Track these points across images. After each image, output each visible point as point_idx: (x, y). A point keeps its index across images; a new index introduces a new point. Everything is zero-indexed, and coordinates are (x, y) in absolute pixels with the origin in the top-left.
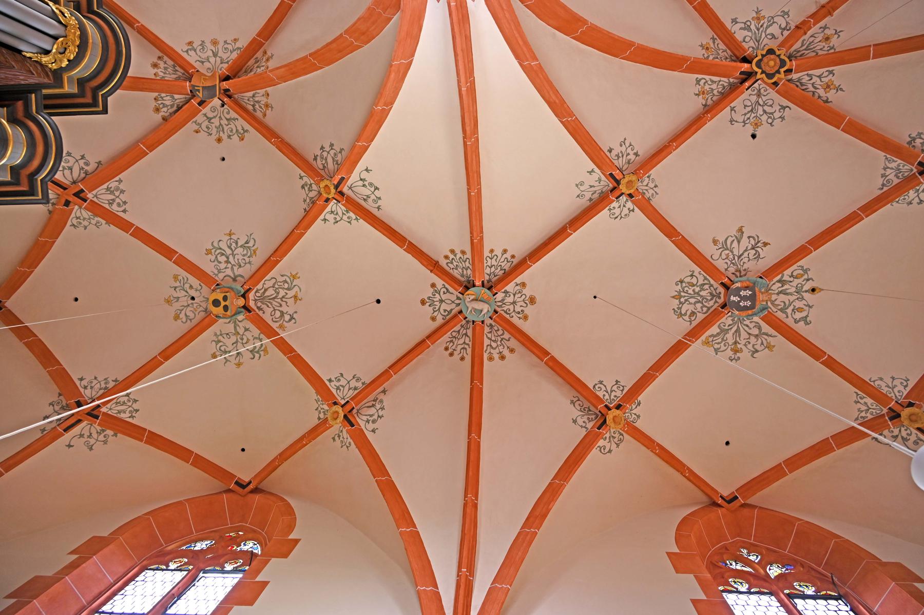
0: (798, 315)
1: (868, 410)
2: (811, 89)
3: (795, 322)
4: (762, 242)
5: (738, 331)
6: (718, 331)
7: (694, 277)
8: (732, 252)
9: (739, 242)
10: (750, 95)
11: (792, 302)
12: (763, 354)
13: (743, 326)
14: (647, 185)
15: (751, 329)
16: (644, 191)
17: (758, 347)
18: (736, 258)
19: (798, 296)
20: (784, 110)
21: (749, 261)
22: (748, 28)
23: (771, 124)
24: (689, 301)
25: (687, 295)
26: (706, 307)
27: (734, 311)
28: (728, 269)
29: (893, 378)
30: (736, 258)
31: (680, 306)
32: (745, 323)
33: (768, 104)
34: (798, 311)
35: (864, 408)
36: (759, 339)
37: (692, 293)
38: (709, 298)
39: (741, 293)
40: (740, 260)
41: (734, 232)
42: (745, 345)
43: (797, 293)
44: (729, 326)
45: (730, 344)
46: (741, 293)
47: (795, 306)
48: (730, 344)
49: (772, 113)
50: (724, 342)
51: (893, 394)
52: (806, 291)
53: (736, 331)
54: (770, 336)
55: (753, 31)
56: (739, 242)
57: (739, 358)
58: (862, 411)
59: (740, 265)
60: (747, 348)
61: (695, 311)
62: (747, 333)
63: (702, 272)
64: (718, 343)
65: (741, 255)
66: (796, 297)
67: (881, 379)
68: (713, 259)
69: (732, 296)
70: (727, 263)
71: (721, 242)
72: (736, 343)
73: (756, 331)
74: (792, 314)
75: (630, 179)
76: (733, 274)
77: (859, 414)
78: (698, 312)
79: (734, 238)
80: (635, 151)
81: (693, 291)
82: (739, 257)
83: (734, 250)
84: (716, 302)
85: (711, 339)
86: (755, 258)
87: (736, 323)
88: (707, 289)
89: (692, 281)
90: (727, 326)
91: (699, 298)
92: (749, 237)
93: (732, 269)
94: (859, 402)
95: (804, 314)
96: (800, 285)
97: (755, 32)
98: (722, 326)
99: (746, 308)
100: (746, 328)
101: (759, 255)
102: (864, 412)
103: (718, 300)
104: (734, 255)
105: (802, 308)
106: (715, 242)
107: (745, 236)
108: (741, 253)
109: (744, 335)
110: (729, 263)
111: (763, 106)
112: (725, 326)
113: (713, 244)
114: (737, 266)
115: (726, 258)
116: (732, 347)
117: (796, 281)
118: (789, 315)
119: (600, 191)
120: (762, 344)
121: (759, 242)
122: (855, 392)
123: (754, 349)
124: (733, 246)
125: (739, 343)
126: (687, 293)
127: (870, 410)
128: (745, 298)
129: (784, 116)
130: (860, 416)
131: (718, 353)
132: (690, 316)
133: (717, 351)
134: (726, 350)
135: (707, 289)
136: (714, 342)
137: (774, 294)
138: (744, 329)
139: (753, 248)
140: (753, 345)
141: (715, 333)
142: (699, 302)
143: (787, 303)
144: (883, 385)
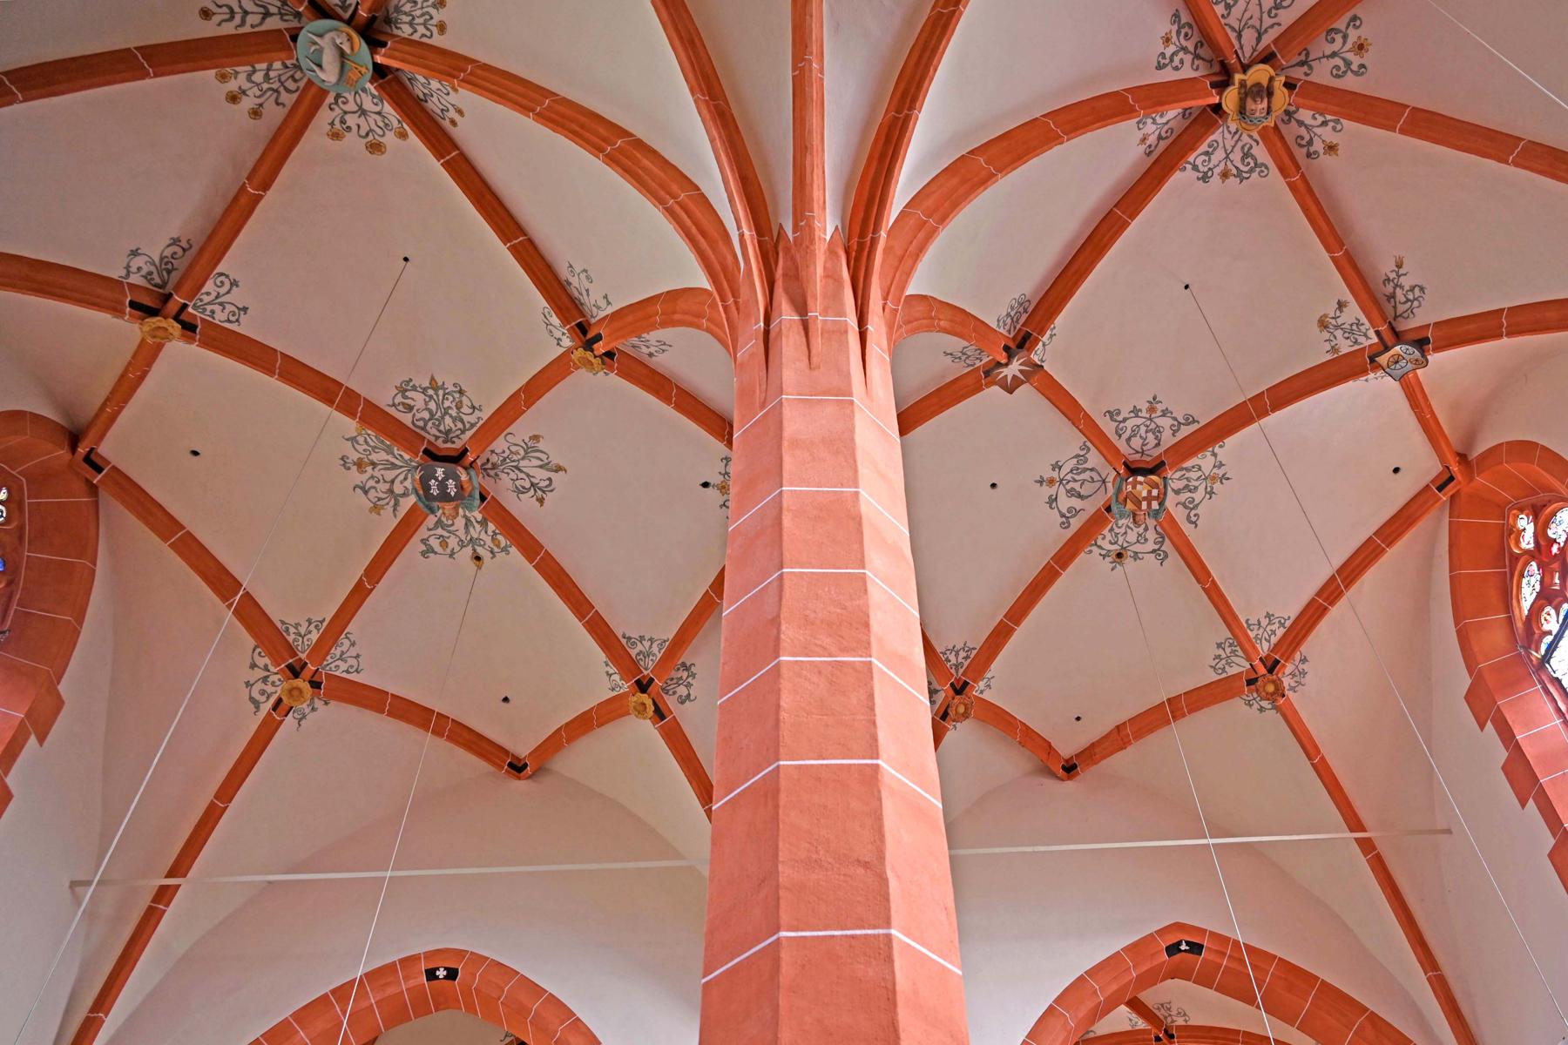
0: (435, 543)
1: (300, 636)
5: (394, 466)
12: (364, 502)
15: (401, 483)
17: (372, 494)
24: (430, 401)
25: (441, 398)
26: (425, 425)
27: (420, 472)
29: (358, 656)
31: (418, 389)
35: (302, 630)
36: (386, 496)
37: (445, 406)
38: (442, 428)
39: (451, 481)
42: (372, 477)
46: (451, 481)
51: (330, 661)
53: (392, 464)
54: (395, 510)
57: (349, 469)
58: (296, 628)
61: (415, 410)
63: (481, 422)
67: (353, 644)
72: (374, 465)
73: (398, 489)
77: (292, 625)
78: (414, 415)
81: (449, 408)
84: (437, 438)
88: (456, 426)
89: (465, 407)
91: (439, 414)
94: (310, 624)
99: (427, 488)
100: (402, 477)
102: (295, 631)
103: (441, 440)
109: (390, 475)
118: (432, 532)
119: (582, 301)
120: (380, 499)
122: (324, 619)
123: (369, 489)
126: (443, 399)
127: (300, 639)
128: (442, 485)
130: (290, 627)
132: (403, 404)
135: (456, 426)
138: (399, 474)
140: (374, 488)
142: (432, 415)
143: (451, 529)
144: (344, 648)
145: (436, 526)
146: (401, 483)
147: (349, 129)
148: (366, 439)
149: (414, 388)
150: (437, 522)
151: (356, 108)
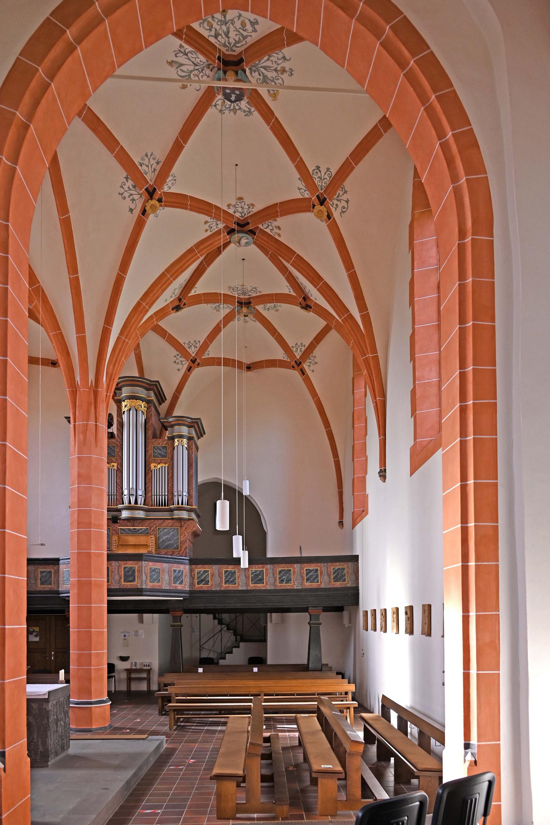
0: (249, 27)
3: (255, 32)
7: (217, 103)
8: (192, 71)
11: (236, 29)
18: (197, 67)
19: (230, 23)
21: (199, 58)
28: (208, 74)
30: (197, 67)
34: (245, 27)
43: (226, 24)
47: (240, 28)
52: (225, 17)
65: (193, 62)
66: (231, 24)
69: (231, 99)
70: (202, 76)
74: (248, 33)
82: (195, 65)
83: (189, 70)
86: (196, 54)
95: (248, 24)
96: (219, 23)
105: (242, 22)
110: (201, 74)
113: (186, 89)
114: (204, 67)
115: (198, 76)
117: (215, 25)
137: (229, 40)
143: (237, 33)
145: (246, 37)
150: (246, 39)
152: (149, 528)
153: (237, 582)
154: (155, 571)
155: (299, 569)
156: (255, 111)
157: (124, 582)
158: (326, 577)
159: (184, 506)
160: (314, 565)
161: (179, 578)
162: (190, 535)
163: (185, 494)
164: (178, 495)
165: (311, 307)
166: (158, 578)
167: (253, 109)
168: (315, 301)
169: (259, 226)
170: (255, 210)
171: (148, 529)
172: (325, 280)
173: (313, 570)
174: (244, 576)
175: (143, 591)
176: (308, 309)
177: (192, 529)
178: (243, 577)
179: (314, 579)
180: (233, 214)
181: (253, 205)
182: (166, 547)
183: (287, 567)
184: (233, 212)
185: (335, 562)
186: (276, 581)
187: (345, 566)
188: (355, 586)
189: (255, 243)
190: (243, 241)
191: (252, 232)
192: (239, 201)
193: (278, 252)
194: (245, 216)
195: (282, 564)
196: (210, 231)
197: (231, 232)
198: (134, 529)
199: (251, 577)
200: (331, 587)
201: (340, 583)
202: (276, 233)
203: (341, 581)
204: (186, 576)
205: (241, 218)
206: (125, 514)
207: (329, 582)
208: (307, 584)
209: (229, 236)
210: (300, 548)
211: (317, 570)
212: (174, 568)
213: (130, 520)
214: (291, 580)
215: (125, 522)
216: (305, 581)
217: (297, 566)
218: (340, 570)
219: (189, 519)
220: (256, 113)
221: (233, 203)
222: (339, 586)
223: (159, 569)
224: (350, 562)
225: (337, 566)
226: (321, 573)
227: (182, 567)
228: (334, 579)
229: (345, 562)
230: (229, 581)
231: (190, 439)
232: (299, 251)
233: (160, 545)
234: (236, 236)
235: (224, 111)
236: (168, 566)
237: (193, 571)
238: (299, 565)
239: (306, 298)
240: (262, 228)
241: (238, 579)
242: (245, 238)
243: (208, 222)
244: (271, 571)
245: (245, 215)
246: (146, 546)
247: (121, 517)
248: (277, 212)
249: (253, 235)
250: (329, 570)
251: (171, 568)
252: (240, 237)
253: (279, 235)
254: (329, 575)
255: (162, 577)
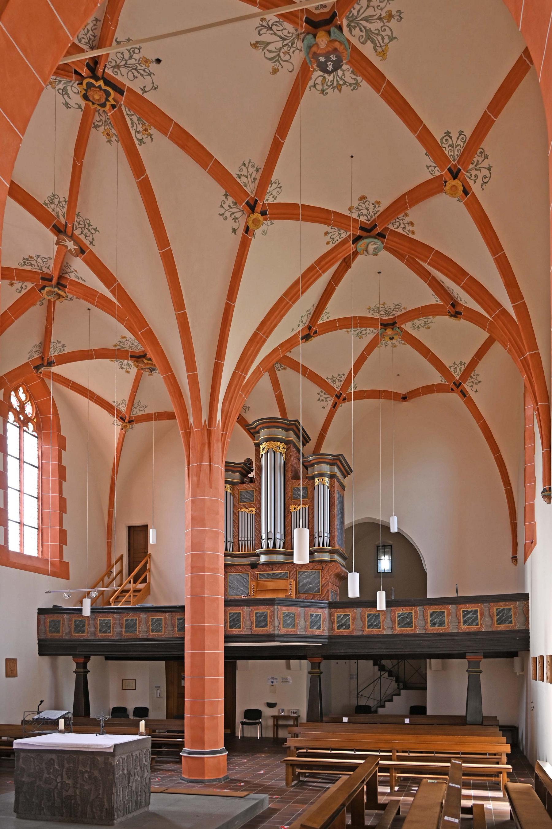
2: (91, 32)
4: (261, 23)
5: (366, 19)
6: (369, 42)
8: (281, 48)
9: (268, 44)
10: (123, 76)
13: (360, 15)
14: (247, 177)
16: (253, 180)
18: (286, 42)
20: (120, 42)
22: (64, 90)
23: (139, 49)
30: (286, 42)
32: (355, 14)
33: (122, 56)
40: (286, 38)
41: (259, 53)
42: (382, 9)
44: (361, 31)
45: (382, 24)
48: (382, 24)
49: (129, 51)
50: (381, 33)
55: (64, 85)
56: (268, 44)
59: (292, 36)
60: (384, 8)
62: (367, 9)
64: (383, 39)
68: (293, 70)
69: (328, 69)
71: (273, 64)
72: (380, 18)
75: (252, 219)
76: (303, 41)
79: (265, 51)
80: (224, 198)
82: (284, 39)
83: (278, 47)
85: (379, 49)
86: (281, 25)
87: (357, 23)
90: (361, 34)
92: (260, 35)
93: (299, 44)
97: (64, 83)
98: (363, 39)
101: (276, 22)
104: (283, 46)
106: (275, 71)
107: (259, 39)
108: (279, 39)
109: (370, 12)
110: (292, 49)
111: (126, 61)
112: (362, 36)
113: (278, 73)
114: (294, 39)
115: (288, 53)
116: (385, 21)
121: (262, 26)
124: (274, 49)
125: (381, 15)
129: (126, 39)
131: (394, 36)
133: (391, 39)
134: (390, 28)
136: (382, 44)
138: (363, 13)
139: (271, 29)
141: (372, 45)
146: (362, 7)
147: (373, 204)
148: (383, 42)
149: (350, 85)
151: (369, 210)
152: (289, 572)
153: (381, 626)
154: (289, 616)
155: (454, 611)
156: (362, 81)
157: (256, 627)
158: (487, 620)
159: (325, 547)
160: (473, 605)
161: (317, 622)
162: (332, 577)
163: (326, 535)
164: (319, 537)
165: (460, 314)
166: (292, 623)
167: (360, 79)
168: (466, 305)
169: (388, 226)
170: (382, 208)
171: (288, 573)
172: (471, 274)
173: (471, 611)
174: (389, 620)
175: (275, 637)
176: (459, 316)
177: (334, 571)
178: (389, 621)
179: (473, 621)
180: (358, 218)
181: (378, 202)
182: (307, 591)
183: (441, 609)
184: (357, 217)
185: (499, 602)
186: (427, 625)
187: (512, 607)
188: (524, 628)
189: (386, 248)
190: (371, 248)
191: (381, 236)
192: (362, 202)
193: (413, 252)
194: (372, 219)
195: (434, 605)
196: (333, 243)
197: (357, 239)
198: (274, 574)
199: (398, 621)
200: (493, 630)
201: (505, 625)
202: (409, 231)
203: (507, 623)
204: (324, 620)
205: (367, 222)
206: (263, 559)
207: (491, 625)
208: (464, 627)
209: (354, 245)
210: (457, 587)
211: (476, 611)
212: (311, 612)
213: (268, 564)
214: (445, 623)
215: (264, 567)
216: (462, 623)
217: (452, 608)
218: (505, 611)
219: (331, 561)
220: (364, 84)
221: (355, 205)
222: (504, 629)
223: (294, 614)
224: (518, 601)
225: (502, 606)
226: (482, 614)
227: (320, 611)
228: (497, 621)
229: (511, 601)
230: (372, 625)
231: (332, 477)
232: (437, 247)
233: (300, 588)
234: (361, 244)
235: (326, 91)
236: (304, 611)
237: (333, 615)
238: (454, 606)
239: (455, 304)
240: (393, 229)
241: (383, 622)
242: (373, 243)
243: (329, 233)
244: (421, 613)
245: (371, 218)
246: (285, 590)
247: (259, 562)
248: (406, 203)
249: (382, 239)
250: (490, 610)
251: (308, 613)
252: (367, 243)
253: (413, 233)
254: (492, 617)
255: (296, 622)
